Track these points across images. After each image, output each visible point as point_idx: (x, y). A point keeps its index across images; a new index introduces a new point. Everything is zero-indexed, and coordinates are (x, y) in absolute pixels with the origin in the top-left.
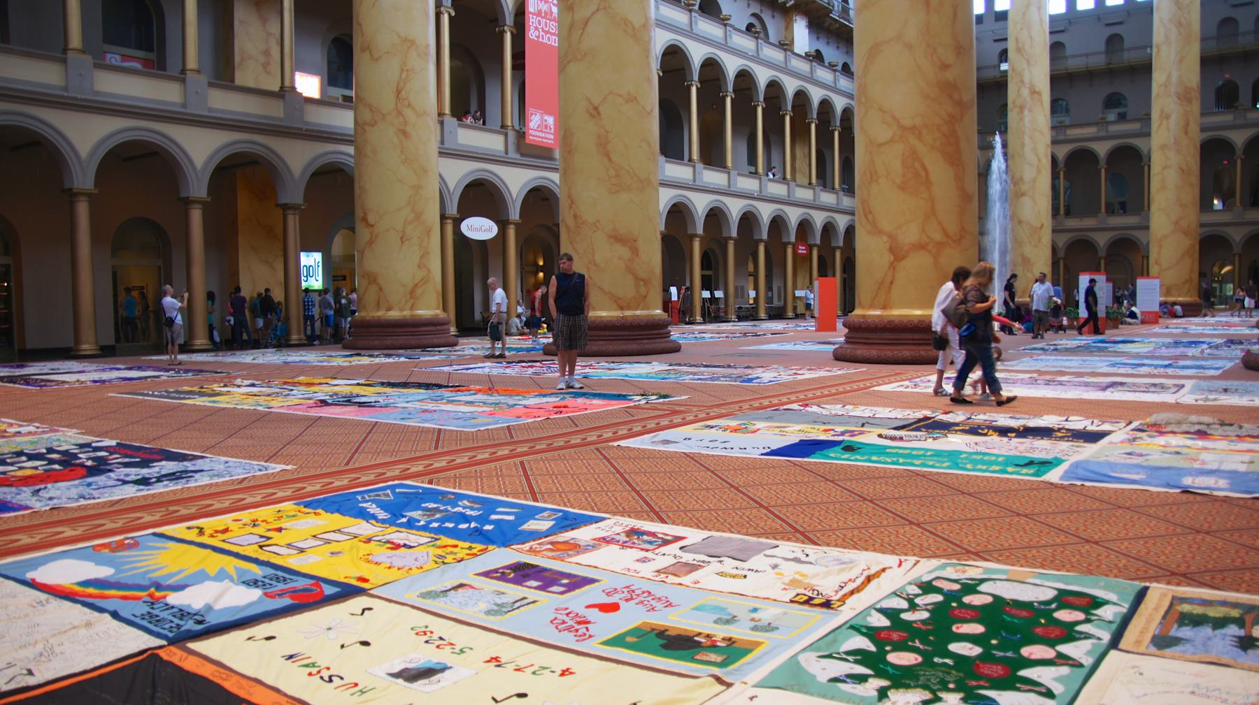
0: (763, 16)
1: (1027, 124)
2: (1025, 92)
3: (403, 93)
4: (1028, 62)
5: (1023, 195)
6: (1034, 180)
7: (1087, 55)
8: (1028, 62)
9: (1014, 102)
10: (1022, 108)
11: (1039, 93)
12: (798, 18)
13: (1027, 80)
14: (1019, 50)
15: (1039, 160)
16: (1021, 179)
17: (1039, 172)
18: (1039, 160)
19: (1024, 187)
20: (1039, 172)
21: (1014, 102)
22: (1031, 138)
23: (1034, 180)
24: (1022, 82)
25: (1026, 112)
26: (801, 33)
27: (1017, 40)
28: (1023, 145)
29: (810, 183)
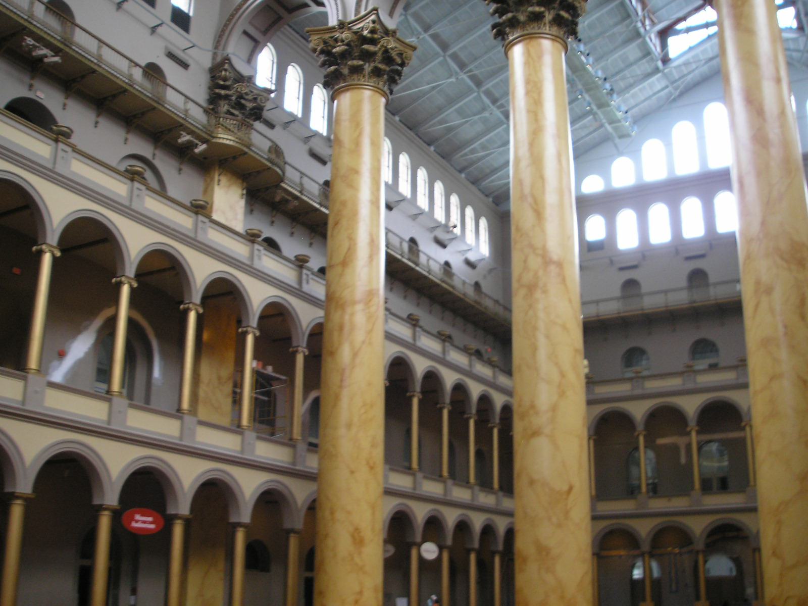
0: (157, 163)
1: (541, 315)
6: (554, 408)
7: (666, 292)
10: (531, 288)
11: (560, 265)
12: (224, 180)
15: (563, 375)
16: (533, 406)
17: (562, 394)
18: (563, 375)
20: (562, 394)
21: (519, 280)
22: (548, 337)
23: (554, 408)
25: (538, 294)
26: (228, 202)
28: (535, 349)
29: (179, 410)
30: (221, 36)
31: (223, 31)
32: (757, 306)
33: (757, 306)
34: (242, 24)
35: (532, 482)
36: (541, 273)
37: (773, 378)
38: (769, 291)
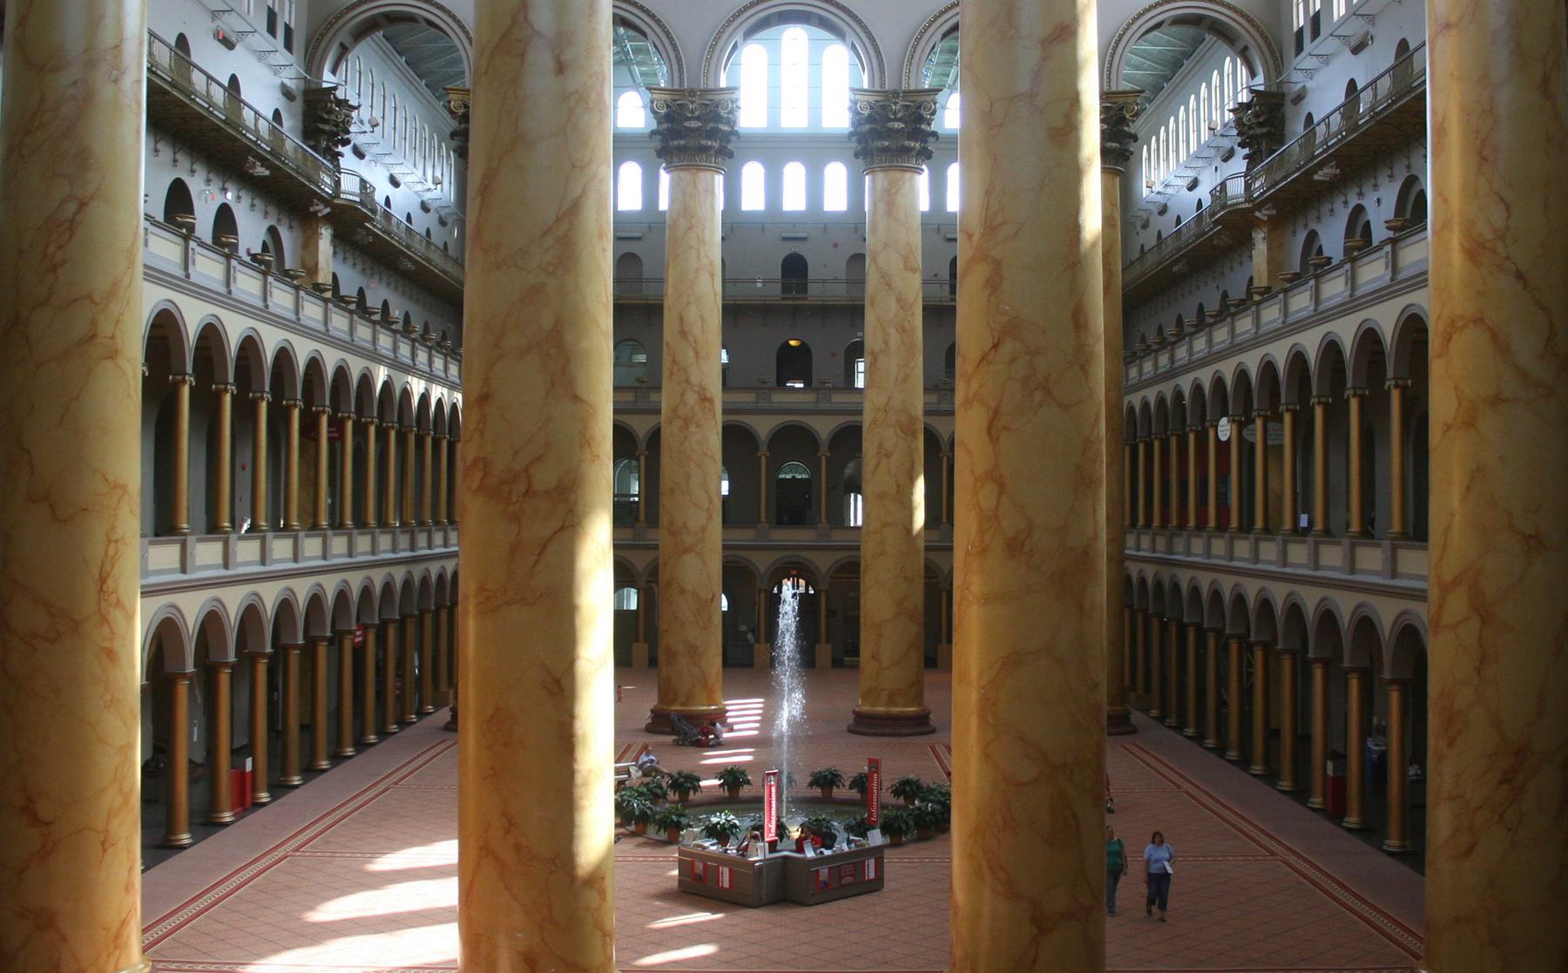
2: (691, 398)
3: (110, 581)
4: (697, 353)
5: (686, 551)
6: (704, 529)
8: (697, 353)
9: (674, 410)
10: (687, 422)
11: (711, 401)
13: (693, 379)
14: (684, 334)
16: (685, 526)
19: (688, 540)
20: (710, 518)
24: (688, 381)
25: (693, 428)
27: (681, 319)
30: (316, 48)
31: (319, 42)
32: (878, 464)
33: (878, 464)
34: (344, 36)
35: (683, 592)
36: (697, 409)
37: (885, 525)
38: (888, 456)
